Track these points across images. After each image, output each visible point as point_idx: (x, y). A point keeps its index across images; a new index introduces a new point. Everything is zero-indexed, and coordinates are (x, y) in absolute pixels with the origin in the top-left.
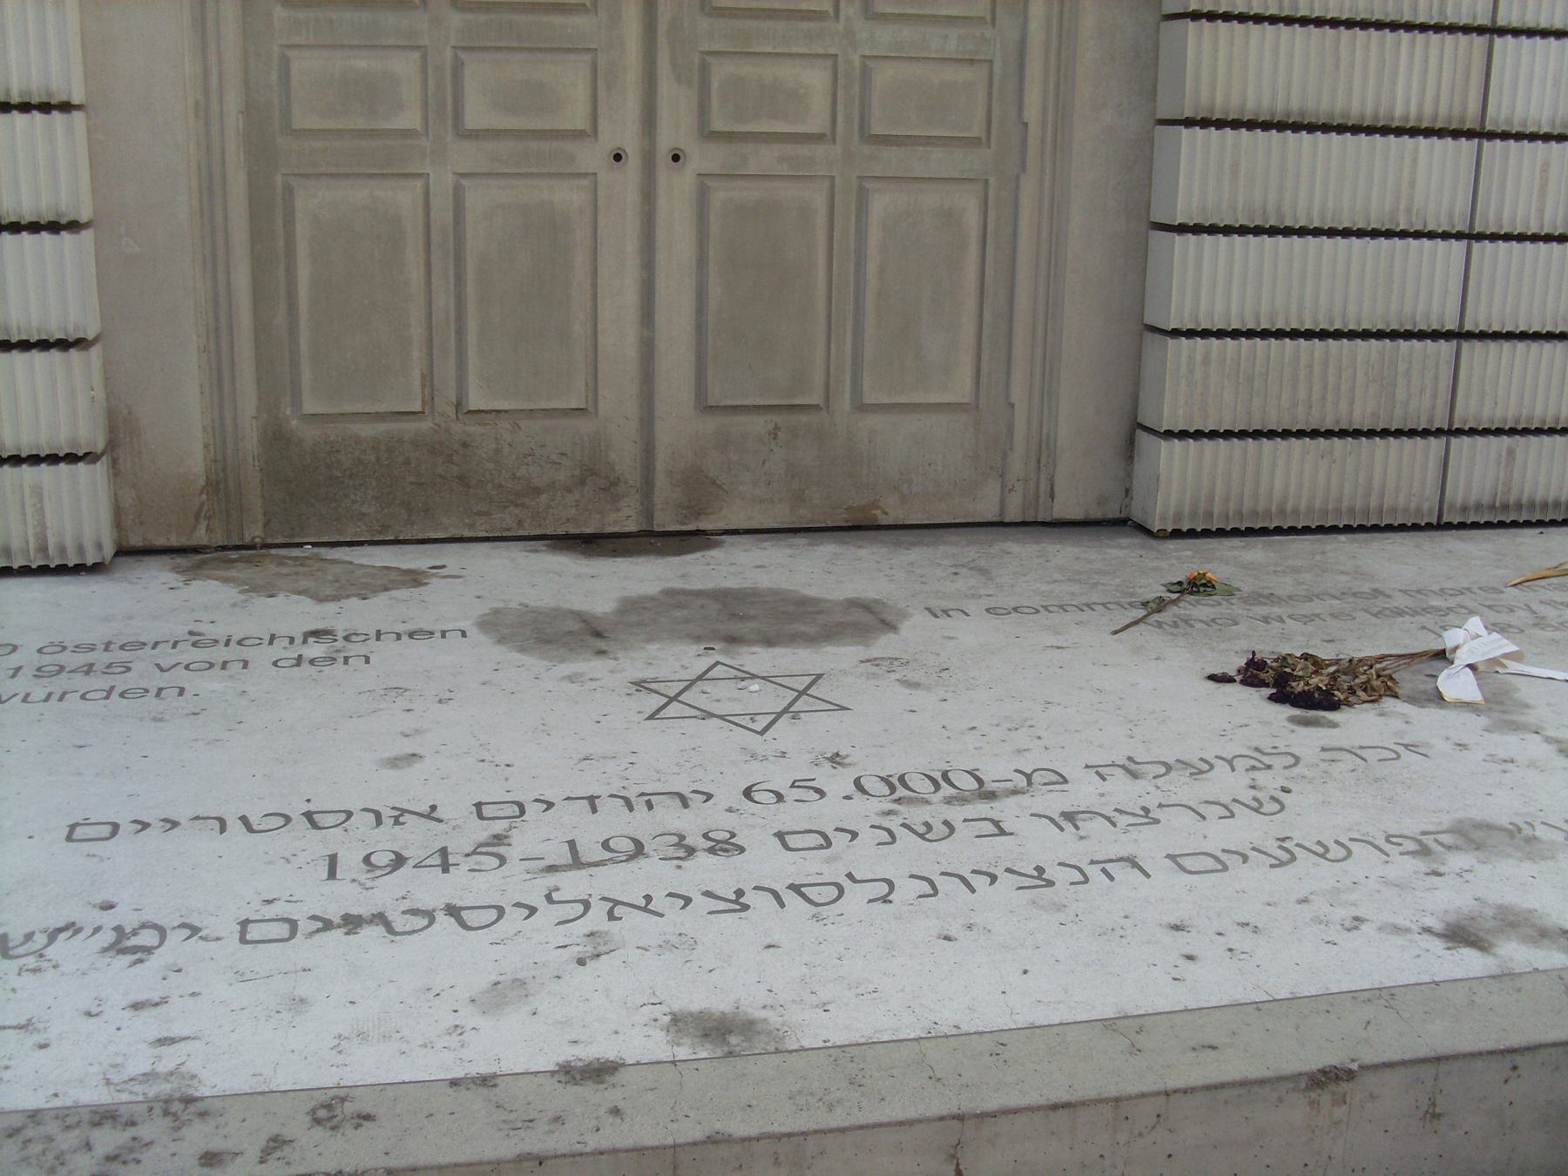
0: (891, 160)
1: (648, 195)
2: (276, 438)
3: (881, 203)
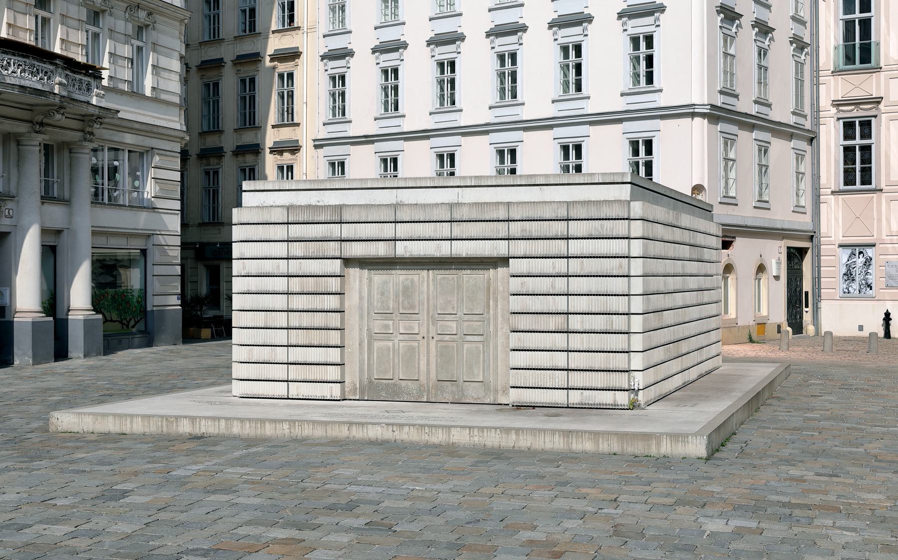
0: (469, 338)
1: (428, 344)
2: (370, 382)
3: (466, 346)
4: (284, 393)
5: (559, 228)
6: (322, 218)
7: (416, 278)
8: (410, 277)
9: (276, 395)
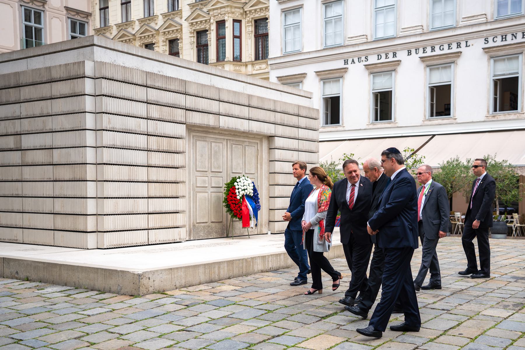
2: (194, 226)
4: (145, 240)
5: (294, 120)
6: (172, 88)
7: (221, 145)
8: (218, 144)
9: (139, 242)
